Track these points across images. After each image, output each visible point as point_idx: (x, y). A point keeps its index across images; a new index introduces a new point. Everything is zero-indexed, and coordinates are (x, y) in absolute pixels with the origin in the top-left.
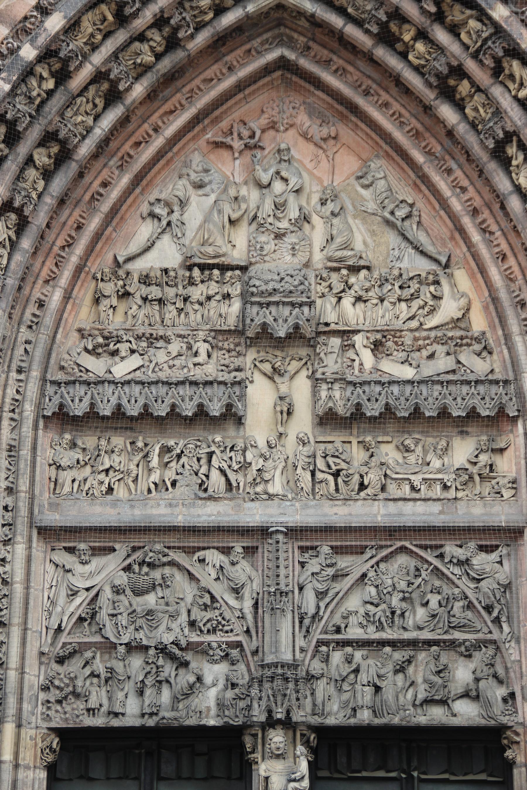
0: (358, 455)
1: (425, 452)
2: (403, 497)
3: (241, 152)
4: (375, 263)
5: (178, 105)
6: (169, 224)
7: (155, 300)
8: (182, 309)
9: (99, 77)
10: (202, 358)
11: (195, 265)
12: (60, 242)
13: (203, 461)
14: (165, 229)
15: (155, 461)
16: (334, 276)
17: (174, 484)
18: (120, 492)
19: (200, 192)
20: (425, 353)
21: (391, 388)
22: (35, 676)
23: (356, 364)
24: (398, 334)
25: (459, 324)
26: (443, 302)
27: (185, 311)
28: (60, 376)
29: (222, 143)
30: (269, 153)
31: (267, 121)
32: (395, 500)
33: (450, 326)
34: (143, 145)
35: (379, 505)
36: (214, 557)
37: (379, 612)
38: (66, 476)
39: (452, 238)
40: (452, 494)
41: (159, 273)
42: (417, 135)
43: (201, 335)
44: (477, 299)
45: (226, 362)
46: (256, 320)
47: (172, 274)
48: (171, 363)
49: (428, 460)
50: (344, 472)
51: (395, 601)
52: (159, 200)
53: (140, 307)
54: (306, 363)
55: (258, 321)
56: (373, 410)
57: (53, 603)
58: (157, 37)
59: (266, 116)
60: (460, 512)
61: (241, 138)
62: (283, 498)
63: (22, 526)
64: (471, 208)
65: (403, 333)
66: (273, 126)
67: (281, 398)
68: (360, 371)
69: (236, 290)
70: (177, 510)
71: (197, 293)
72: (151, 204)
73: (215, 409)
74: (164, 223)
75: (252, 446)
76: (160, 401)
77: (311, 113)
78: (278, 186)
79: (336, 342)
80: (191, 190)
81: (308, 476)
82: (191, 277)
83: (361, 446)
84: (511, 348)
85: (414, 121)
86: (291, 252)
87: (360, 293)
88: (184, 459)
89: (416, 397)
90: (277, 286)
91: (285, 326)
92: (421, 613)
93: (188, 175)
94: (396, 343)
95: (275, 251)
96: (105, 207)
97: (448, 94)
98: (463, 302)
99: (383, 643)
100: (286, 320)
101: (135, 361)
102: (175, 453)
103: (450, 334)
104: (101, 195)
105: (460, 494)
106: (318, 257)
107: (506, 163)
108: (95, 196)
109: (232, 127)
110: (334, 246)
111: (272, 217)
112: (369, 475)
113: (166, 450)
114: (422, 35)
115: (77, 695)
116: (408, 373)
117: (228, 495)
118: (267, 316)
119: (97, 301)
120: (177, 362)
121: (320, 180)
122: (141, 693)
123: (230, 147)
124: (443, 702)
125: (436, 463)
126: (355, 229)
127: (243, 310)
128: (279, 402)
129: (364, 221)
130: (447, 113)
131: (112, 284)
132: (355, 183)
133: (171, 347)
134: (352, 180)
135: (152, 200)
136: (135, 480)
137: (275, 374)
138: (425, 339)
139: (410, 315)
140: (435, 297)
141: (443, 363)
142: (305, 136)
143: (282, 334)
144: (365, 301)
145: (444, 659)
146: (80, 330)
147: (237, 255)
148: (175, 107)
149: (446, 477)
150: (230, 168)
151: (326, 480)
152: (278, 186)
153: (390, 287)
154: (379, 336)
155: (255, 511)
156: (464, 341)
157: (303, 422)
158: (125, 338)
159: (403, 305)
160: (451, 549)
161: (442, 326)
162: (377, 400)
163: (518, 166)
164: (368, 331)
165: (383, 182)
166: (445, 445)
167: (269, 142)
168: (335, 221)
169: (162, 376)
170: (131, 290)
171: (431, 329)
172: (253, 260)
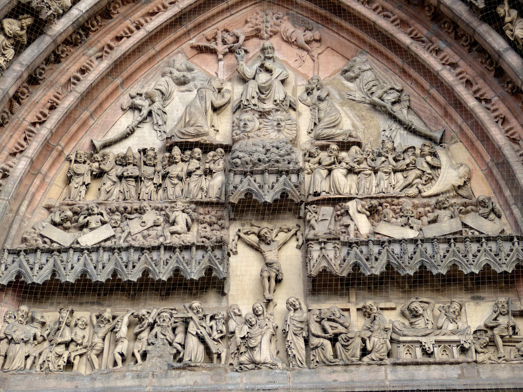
0: (357, 323)
1: (436, 318)
2: (415, 360)
3: (225, 55)
4: (364, 142)
5: (161, 7)
6: (150, 113)
7: (131, 177)
10: (180, 226)
11: (176, 144)
12: (31, 118)
13: (180, 329)
14: (145, 119)
15: (123, 331)
16: (323, 155)
17: (144, 356)
18: (81, 367)
19: (183, 88)
20: (425, 219)
21: (391, 247)
23: (352, 228)
24: (396, 201)
25: (460, 192)
26: (442, 171)
27: (163, 186)
29: (206, 47)
30: (253, 56)
31: (251, 29)
32: (405, 364)
33: (452, 194)
34: (125, 39)
35: (386, 370)
38: (19, 351)
39: (446, 114)
40: (472, 356)
41: (137, 155)
42: (403, 24)
43: (180, 205)
44: (478, 168)
45: (209, 234)
46: (240, 187)
47: (151, 153)
48: (146, 232)
49: (440, 325)
50: (343, 336)
52: (141, 95)
53: (115, 182)
54: (296, 234)
55: (243, 187)
59: (250, 25)
60: (483, 376)
61: (224, 42)
62: (273, 366)
64: (465, 80)
65: (401, 200)
66: (257, 34)
67: (269, 265)
68: (356, 235)
70: (146, 381)
72: (132, 98)
74: (145, 112)
75: (235, 314)
76: (130, 266)
78: (263, 77)
79: (327, 210)
80: (173, 87)
81: (301, 343)
82: (171, 157)
83: (360, 313)
85: (397, 11)
86: (276, 128)
87: (352, 164)
88: (156, 329)
89: (421, 256)
90: (262, 157)
91: (271, 191)
93: (171, 73)
94: (394, 211)
95: (259, 129)
96: (82, 87)
98: (462, 170)
100: (273, 187)
101: (106, 232)
102: (146, 322)
103: (453, 201)
104: (78, 80)
105: (480, 358)
106: (305, 140)
107: (498, 24)
108: (72, 80)
109: (216, 34)
110: (321, 125)
111: (256, 99)
112: (373, 339)
117: (208, 365)
119: (69, 180)
120: (153, 233)
121: (305, 76)
123: (213, 52)
125: (452, 326)
126: (343, 115)
128: (266, 268)
129: (352, 108)
132: (342, 78)
133: (145, 217)
134: (338, 76)
135: (133, 94)
136: (100, 355)
138: (425, 206)
139: (407, 183)
140: (433, 167)
141: (447, 225)
142: (288, 41)
143: (269, 199)
144: (358, 173)
146: (49, 208)
147: (221, 137)
148: (159, 9)
149: (462, 339)
150: (213, 70)
151: (322, 345)
153: (383, 159)
154: (375, 202)
155: (239, 380)
156: (469, 208)
157: (293, 287)
158: (96, 211)
159: (399, 175)
161: (443, 193)
162: (376, 259)
163: (511, 22)
164: (361, 199)
165: (369, 73)
166: (458, 308)
167: (254, 46)
168: (323, 105)
169: (136, 244)
170: (106, 168)
171: (430, 197)
172: (236, 137)
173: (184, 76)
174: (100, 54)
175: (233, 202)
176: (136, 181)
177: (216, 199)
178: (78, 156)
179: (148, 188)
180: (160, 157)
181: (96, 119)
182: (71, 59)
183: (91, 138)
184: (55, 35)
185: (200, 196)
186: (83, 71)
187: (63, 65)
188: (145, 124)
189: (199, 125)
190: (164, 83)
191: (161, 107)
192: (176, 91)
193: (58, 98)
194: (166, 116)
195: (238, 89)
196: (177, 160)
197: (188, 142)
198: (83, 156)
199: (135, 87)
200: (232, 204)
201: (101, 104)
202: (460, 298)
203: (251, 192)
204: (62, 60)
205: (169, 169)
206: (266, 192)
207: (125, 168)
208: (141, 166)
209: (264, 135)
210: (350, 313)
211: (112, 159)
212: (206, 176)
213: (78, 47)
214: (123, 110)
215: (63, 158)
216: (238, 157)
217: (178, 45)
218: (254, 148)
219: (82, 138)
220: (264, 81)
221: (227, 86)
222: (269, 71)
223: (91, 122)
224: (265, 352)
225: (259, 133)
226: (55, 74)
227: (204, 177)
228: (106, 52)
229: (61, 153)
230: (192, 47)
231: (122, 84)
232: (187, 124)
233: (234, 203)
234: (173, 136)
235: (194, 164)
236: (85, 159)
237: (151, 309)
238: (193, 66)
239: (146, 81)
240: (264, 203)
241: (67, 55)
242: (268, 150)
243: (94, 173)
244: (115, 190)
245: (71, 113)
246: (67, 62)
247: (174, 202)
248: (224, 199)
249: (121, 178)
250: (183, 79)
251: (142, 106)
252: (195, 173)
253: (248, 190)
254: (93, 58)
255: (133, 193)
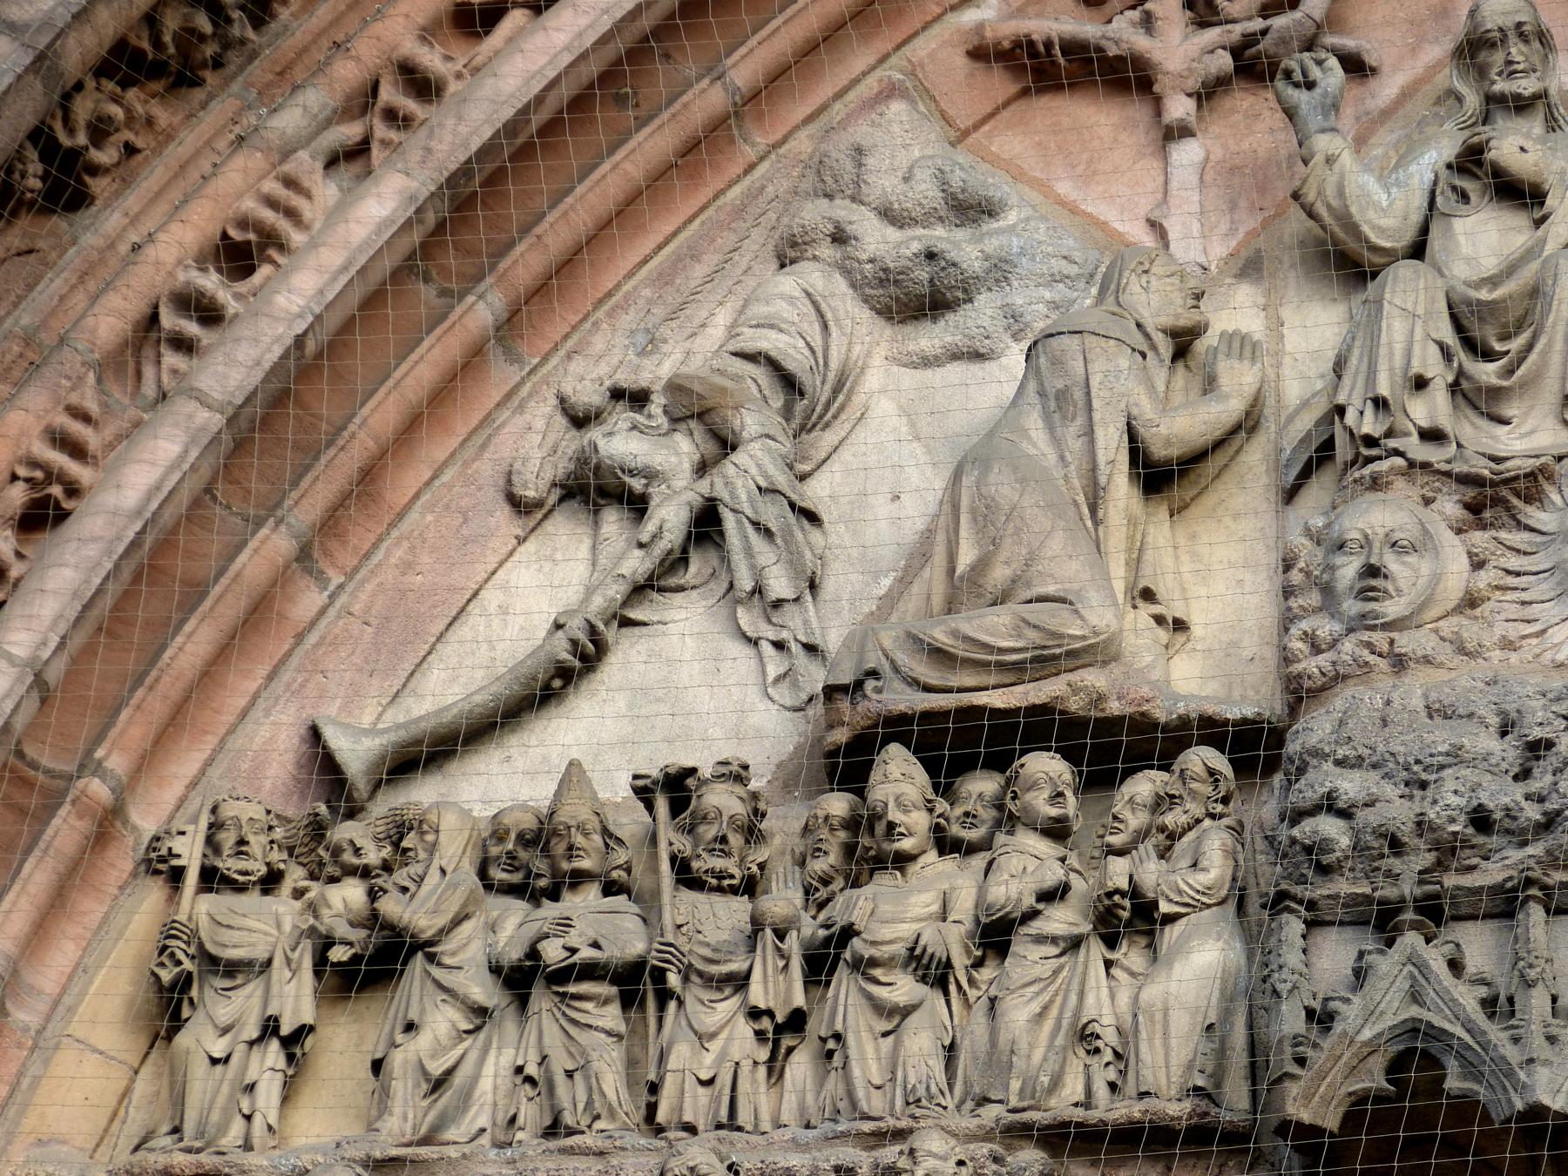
3: (1209, 93)
6: (706, 524)
7: (590, 971)
8: (797, 1021)
11: (897, 727)
14: (677, 561)
27: (816, 1026)
29: (1075, 49)
30: (1406, 95)
41: (631, 820)
46: (1350, 1014)
47: (722, 800)
52: (638, 399)
55: (1376, 1014)
71: (915, 906)
72: (580, 421)
74: (670, 516)
78: (1482, 239)
90: (1500, 795)
93: (839, 237)
95: (1471, 602)
96: (235, 366)
104: (210, 314)
111: (1439, 395)
119: (168, 1008)
123: (1128, 78)
131: (284, 909)
135: (589, 394)
170: (416, 913)
172: (1312, 665)
173: (931, 256)
174: (351, 132)
175: (1306, 1117)
176: (629, 1000)
177: (1187, 1106)
178: (228, 839)
179: (715, 1046)
180: (784, 823)
181: (336, 579)
182: (154, 175)
183: (309, 713)
184: (46, 23)
185: (1073, 1088)
186: (239, 255)
187: (106, 222)
188: (678, 598)
189: (1051, 589)
190: (796, 309)
191: (782, 480)
192: (877, 360)
193: (77, 450)
194: (815, 535)
195: (1313, 326)
196: (906, 844)
197: (976, 711)
198: (257, 843)
199: (598, 343)
200: (1305, 1135)
201: (369, 477)
203: (1435, 1048)
204: (98, 185)
205: (855, 906)
206: (1538, 1044)
207: (550, 910)
208: (656, 893)
209: (1508, 645)
211: (454, 849)
212: (1111, 942)
213: (199, 94)
214: (519, 505)
215: (122, 860)
216: (1329, 805)
217: (882, 45)
218: (1441, 738)
219: (244, 714)
220: (1490, 264)
221: (1236, 312)
222: (1520, 194)
223: (308, 600)
225: (1470, 630)
226: (52, 286)
227: (1096, 951)
228: (391, 115)
229: (107, 825)
230: (980, 54)
231: (510, 328)
232: (964, 590)
233: (1315, 1130)
234: (873, 674)
235: (1027, 863)
236: (276, 856)
238: (995, 185)
239: (672, 298)
240: (1523, 1116)
241: (130, 150)
242: (1537, 748)
243: (338, 954)
244: (489, 1069)
245: (166, 544)
246: (132, 200)
247: (900, 1135)
248: (1244, 1103)
249: (521, 978)
250: (923, 274)
251: (650, 475)
252: (1035, 927)
253: (1413, 1029)
254: (306, 164)
255: (612, 1082)
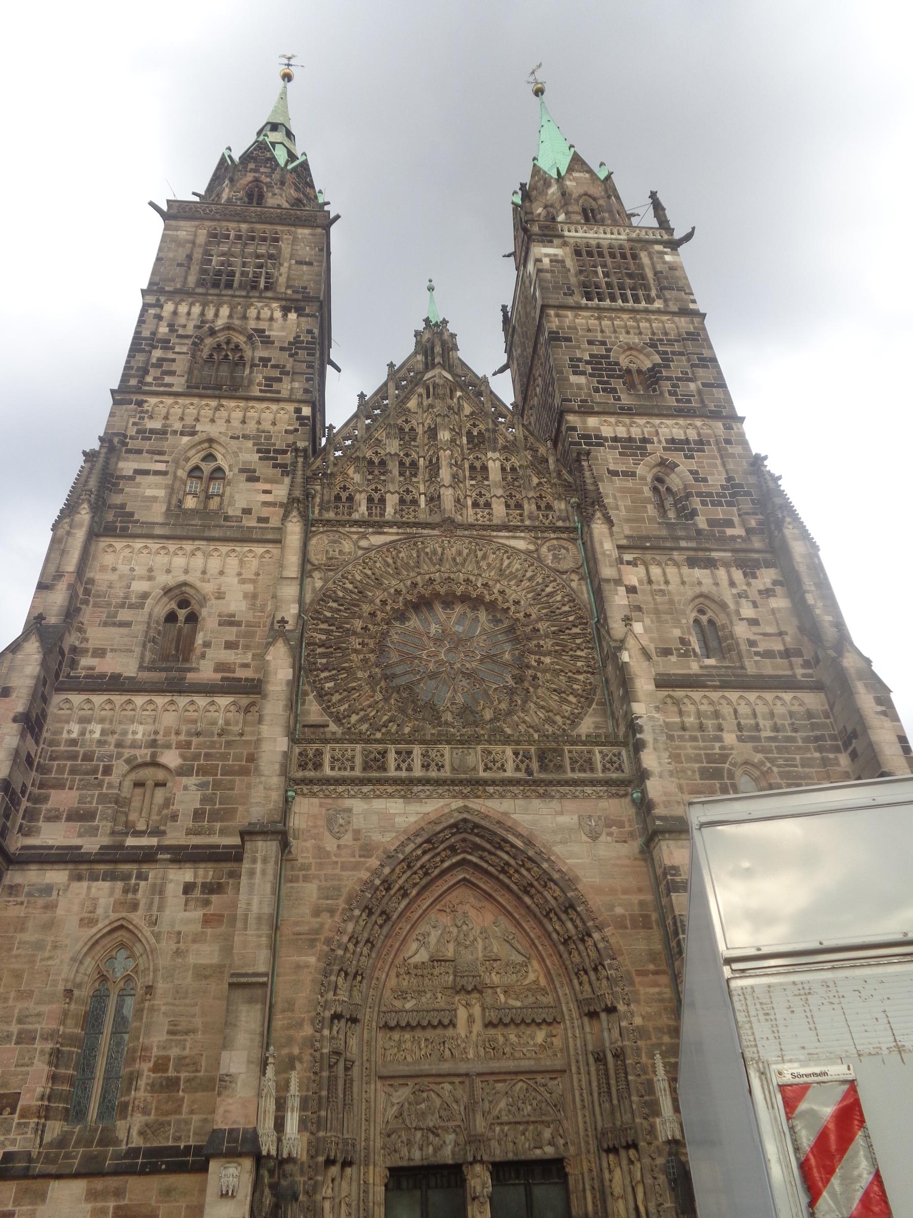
0: (501, 1039)
9: (401, 888)
15: (423, 1045)
22: (379, 1145)
28: (383, 1009)
36: (447, 1087)
37: (513, 1109)
51: (520, 1104)
56: (506, 1020)
57: (385, 1110)
58: (421, 872)
63: (373, 1077)
66: (461, 903)
69: (451, 971)
71: (436, 972)
73: (446, 1022)
77: (475, 897)
78: (465, 927)
79: (490, 991)
84: (557, 992)
92: (529, 1108)
97: (527, 892)
99: (516, 1123)
101: (413, 1002)
106: (480, 955)
113: (426, 1040)
114: (517, 871)
115: (395, 1151)
116: (519, 1004)
118: (464, 981)
122: (421, 1149)
124: (541, 1148)
127: (455, 980)
130: (527, 900)
137: (468, 1005)
141: (531, 999)
145: (539, 1127)
147: (450, 954)
150: (446, 920)
152: (465, 927)
157: (478, 1027)
160: (539, 1078)
195: (455, 930)
202: (534, 1028)
210: (497, 1034)
224: (471, 1056)
237: (430, 1034)
